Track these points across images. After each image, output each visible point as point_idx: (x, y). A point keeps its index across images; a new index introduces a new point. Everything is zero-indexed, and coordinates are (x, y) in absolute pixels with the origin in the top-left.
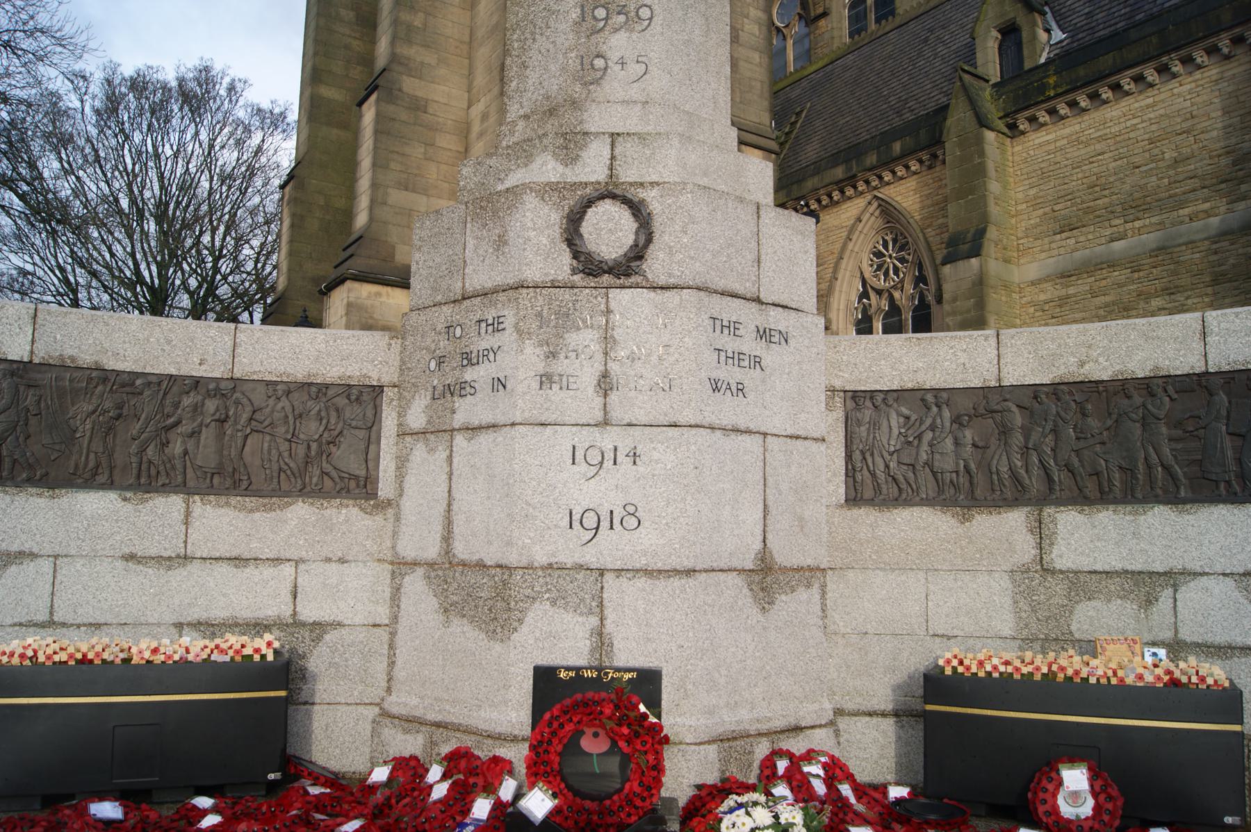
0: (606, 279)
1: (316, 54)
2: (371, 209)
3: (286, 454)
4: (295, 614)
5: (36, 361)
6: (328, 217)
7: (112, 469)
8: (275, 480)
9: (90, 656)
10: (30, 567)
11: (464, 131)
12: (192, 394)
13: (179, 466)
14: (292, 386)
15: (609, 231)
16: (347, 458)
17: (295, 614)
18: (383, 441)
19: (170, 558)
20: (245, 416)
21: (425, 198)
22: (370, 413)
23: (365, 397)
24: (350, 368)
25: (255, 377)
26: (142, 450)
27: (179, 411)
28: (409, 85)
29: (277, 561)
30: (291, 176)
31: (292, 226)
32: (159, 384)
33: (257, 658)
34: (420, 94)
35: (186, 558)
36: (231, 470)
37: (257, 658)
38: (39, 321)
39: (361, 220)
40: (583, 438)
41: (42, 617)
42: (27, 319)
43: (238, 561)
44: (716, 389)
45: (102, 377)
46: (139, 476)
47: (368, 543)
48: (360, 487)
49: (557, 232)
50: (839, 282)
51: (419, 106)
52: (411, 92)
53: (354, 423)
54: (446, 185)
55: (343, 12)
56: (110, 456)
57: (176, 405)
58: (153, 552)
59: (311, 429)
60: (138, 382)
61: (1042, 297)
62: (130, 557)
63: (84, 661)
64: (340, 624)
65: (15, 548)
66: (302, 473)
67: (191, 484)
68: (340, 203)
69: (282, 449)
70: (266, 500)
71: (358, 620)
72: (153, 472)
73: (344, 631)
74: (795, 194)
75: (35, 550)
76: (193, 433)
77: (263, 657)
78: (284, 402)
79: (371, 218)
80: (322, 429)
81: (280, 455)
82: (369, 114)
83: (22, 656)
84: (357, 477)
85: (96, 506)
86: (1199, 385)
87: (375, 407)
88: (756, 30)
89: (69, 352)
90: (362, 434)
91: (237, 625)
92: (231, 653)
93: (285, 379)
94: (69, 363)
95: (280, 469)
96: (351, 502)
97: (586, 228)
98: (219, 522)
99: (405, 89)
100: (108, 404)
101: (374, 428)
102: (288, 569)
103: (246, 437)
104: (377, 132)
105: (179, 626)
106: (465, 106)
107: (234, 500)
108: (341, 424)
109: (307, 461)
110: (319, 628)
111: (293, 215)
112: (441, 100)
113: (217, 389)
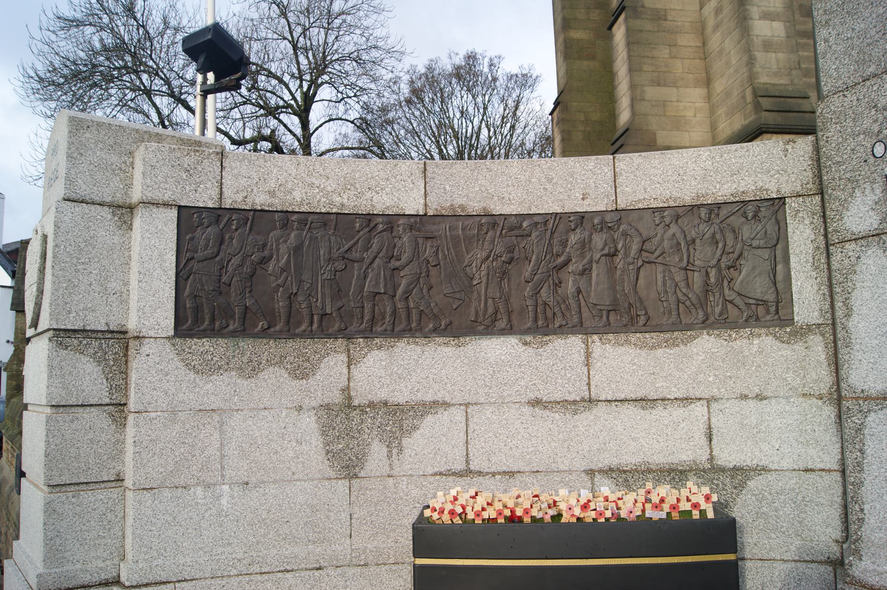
1: (563, 8)
2: (632, 106)
3: (682, 285)
4: (711, 458)
5: (430, 213)
6: (588, 129)
7: (509, 313)
8: (674, 313)
9: (519, 512)
10: (444, 416)
11: (701, 29)
12: (578, 231)
13: (574, 306)
14: (680, 211)
16: (752, 280)
17: (711, 458)
18: (793, 259)
19: (574, 402)
20: (635, 248)
21: (674, 90)
22: (771, 228)
23: (764, 212)
24: (743, 183)
25: (641, 206)
26: (536, 293)
27: (567, 250)
29: (686, 400)
30: (557, 103)
31: (563, 140)
32: (546, 223)
33: (696, 514)
34: (659, 6)
35: (591, 401)
36: (626, 305)
37: (696, 514)
38: (429, 174)
39: (624, 117)
41: (460, 466)
42: (418, 174)
43: (644, 402)
45: (491, 222)
46: (536, 320)
47: (790, 376)
48: (771, 311)
52: (652, 6)
53: (755, 243)
54: (691, 76)
56: (507, 301)
57: (564, 243)
58: (558, 396)
59: (703, 255)
60: (525, 224)
62: (536, 403)
63: (513, 519)
64: (765, 469)
65: (429, 398)
66: (703, 303)
67: (587, 324)
69: (677, 279)
70: (668, 335)
71: (785, 465)
72: (549, 314)
73: (771, 477)
75: (448, 399)
76: (584, 270)
77: (703, 513)
78: (674, 228)
79: (633, 114)
80: (719, 252)
81: (677, 285)
82: (619, 32)
83: (452, 513)
84: (765, 303)
85: (499, 350)
87: (778, 222)
89: (459, 201)
90: (766, 254)
91: (650, 471)
92: (666, 507)
93: (672, 204)
94: (459, 212)
95: (679, 301)
96: (763, 331)
98: (621, 362)
99: (647, 5)
100: (499, 249)
101: (779, 246)
102: (699, 409)
103: (639, 269)
104: (629, 44)
105: (591, 473)
106: (698, 8)
107: (633, 337)
108: (739, 246)
109: (707, 289)
110: (741, 474)
111: (562, 132)
112: (677, 7)
113: (603, 222)
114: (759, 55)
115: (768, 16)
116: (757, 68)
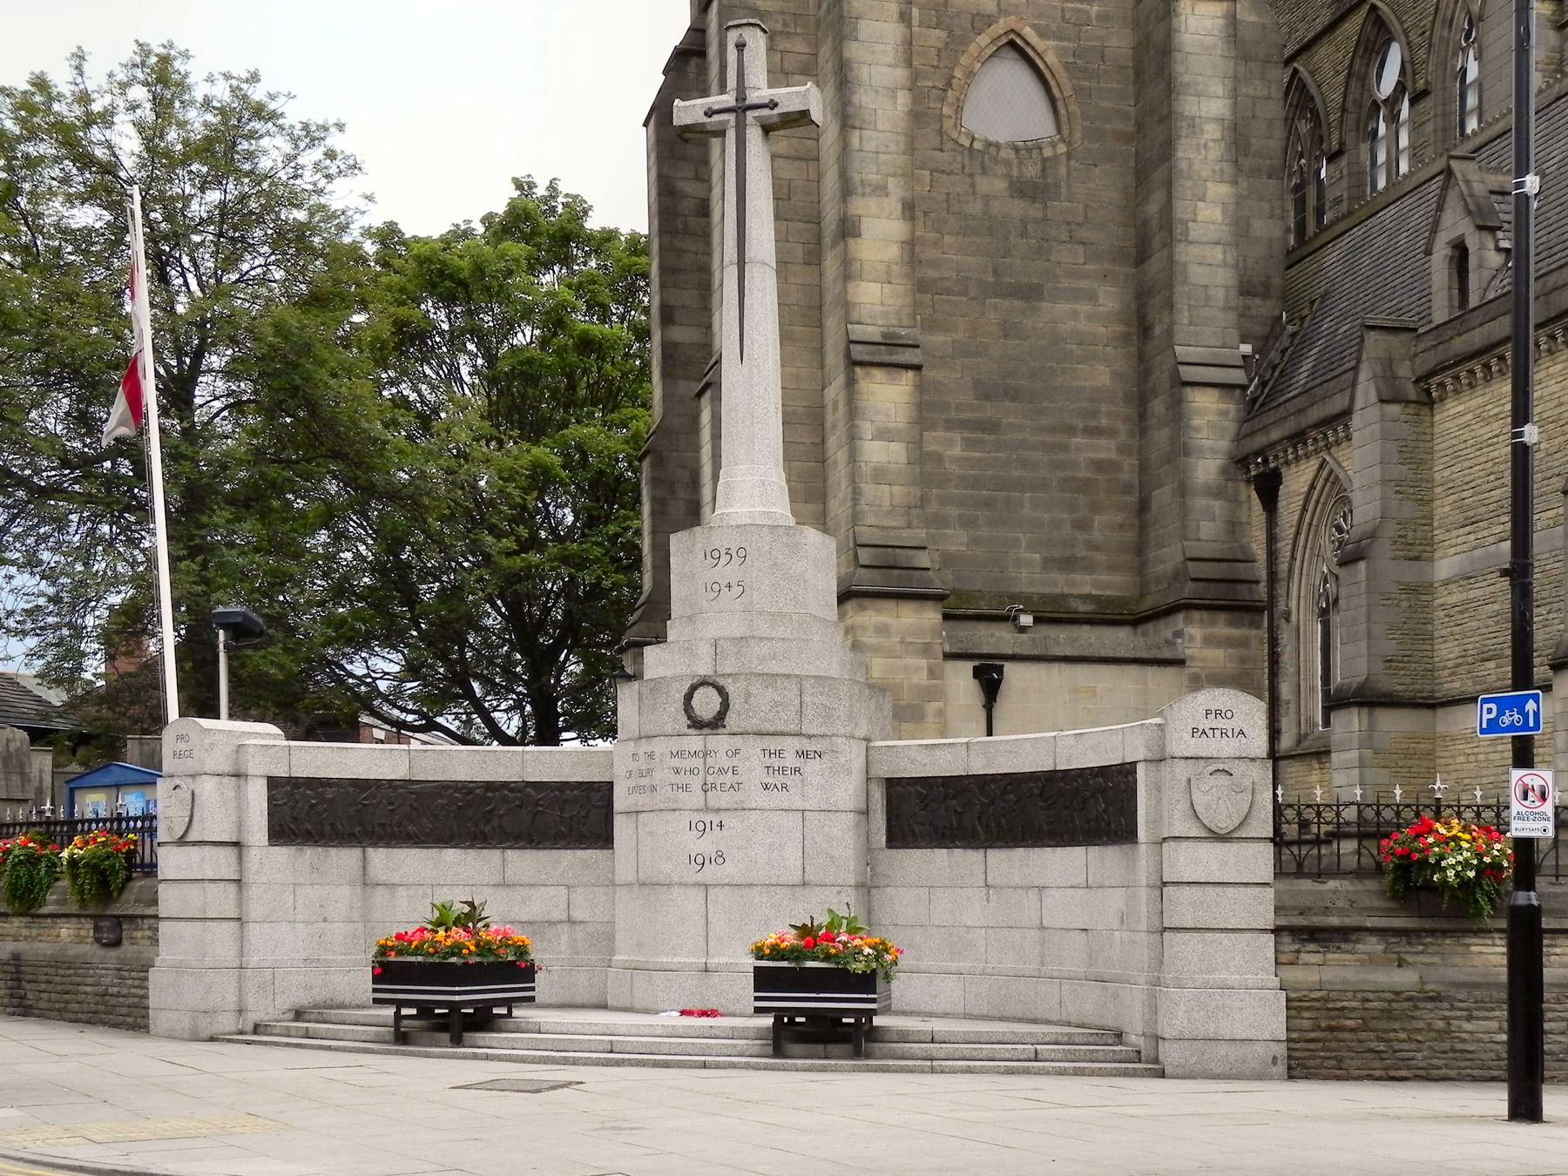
0: (706, 731)
15: (706, 702)
40: (696, 817)
44: (766, 788)
49: (680, 704)
50: (1298, 563)
74: (1260, 441)
97: (694, 702)
114: (868, 489)
115: (883, 435)
116: (863, 506)
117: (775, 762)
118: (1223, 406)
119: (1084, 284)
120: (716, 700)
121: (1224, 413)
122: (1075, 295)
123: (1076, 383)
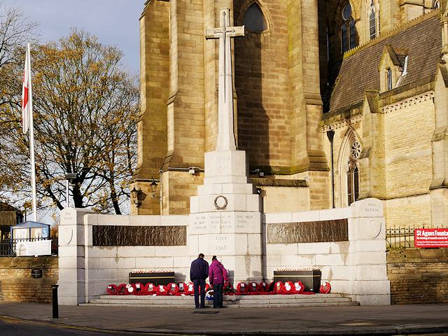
15: (221, 203)
21: (192, 139)
28: (184, 99)
34: (188, 102)
39: (171, 148)
43: (164, 257)
51: (188, 106)
55: (155, 50)
61: (391, 170)
68: (160, 128)
79: (175, 149)
86: (318, 223)
88: (313, 55)
104: (175, 118)
117: (241, 219)
118: (317, 111)
119: (275, 74)
120: (224, 203)
121: (317, 113)
122: (273, 77)
123: (274, 103)
